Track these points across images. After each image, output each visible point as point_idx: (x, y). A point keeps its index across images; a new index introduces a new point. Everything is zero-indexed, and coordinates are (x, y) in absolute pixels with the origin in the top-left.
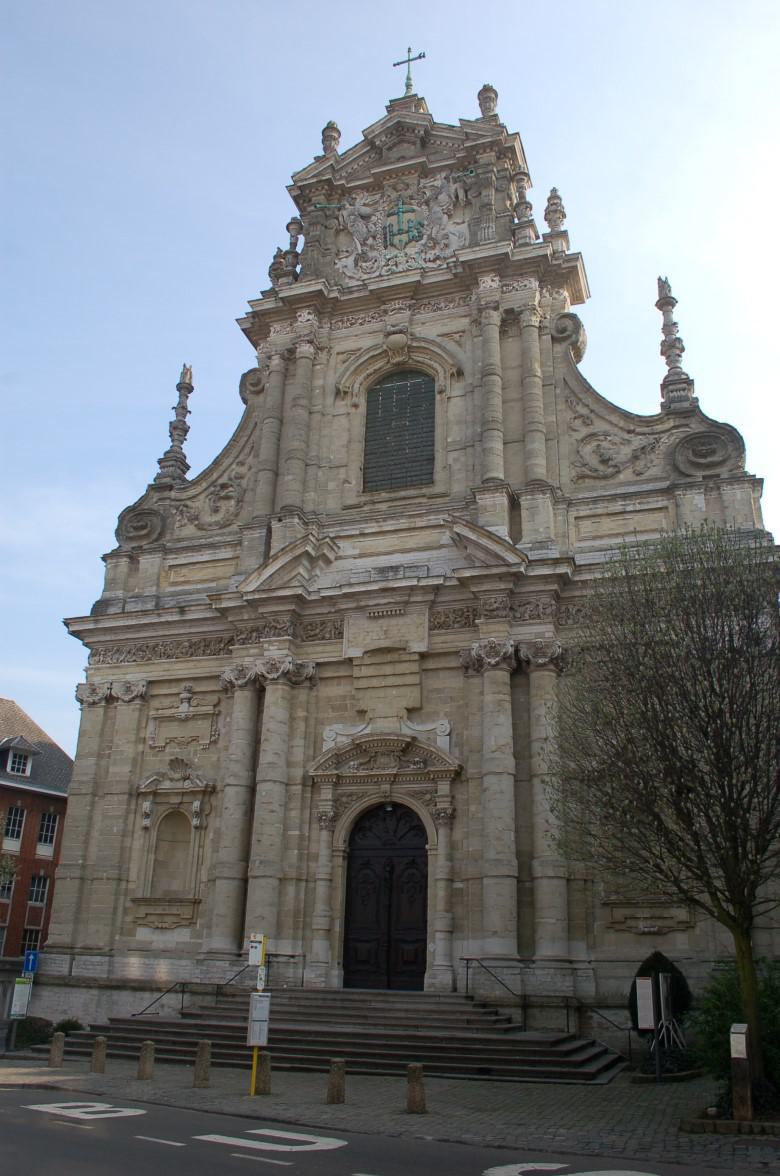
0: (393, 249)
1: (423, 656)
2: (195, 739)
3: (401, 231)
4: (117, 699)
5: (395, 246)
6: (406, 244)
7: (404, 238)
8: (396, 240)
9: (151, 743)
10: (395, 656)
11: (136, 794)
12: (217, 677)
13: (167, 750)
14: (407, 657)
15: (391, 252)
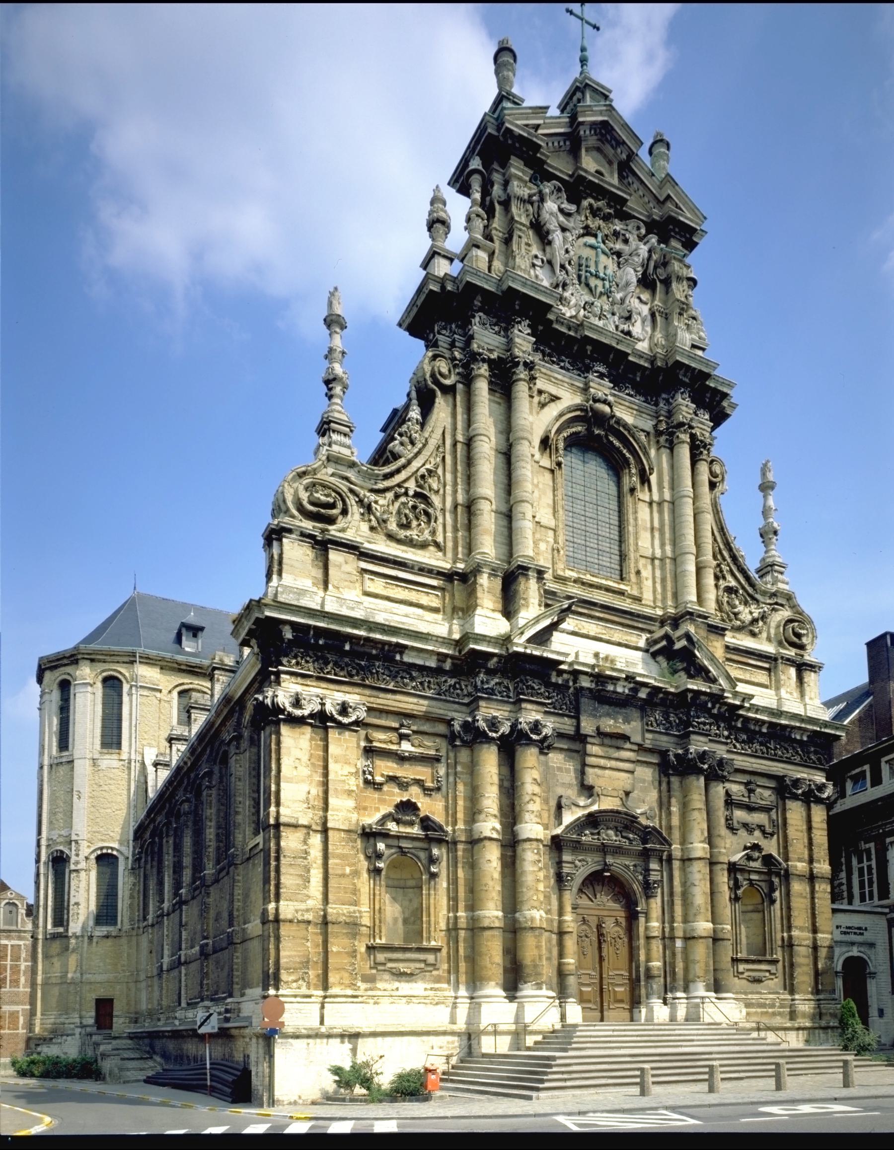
0: (586, 290)
1: (641, 748)
2: (419, 783)
3: (597, 276)
4: (332, 719)
5: (591, 290)
6: (601, 294)
7: (599, 283)
8: (593, 282)
9: (370, 777)
10: (620, 743)
11: (368, 835)
12: (449, 723)
13: (385, 788)
14: (628, 746)
15: (587, 298)
